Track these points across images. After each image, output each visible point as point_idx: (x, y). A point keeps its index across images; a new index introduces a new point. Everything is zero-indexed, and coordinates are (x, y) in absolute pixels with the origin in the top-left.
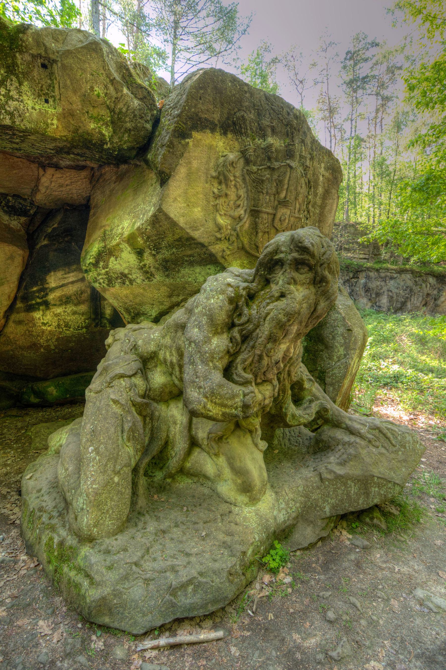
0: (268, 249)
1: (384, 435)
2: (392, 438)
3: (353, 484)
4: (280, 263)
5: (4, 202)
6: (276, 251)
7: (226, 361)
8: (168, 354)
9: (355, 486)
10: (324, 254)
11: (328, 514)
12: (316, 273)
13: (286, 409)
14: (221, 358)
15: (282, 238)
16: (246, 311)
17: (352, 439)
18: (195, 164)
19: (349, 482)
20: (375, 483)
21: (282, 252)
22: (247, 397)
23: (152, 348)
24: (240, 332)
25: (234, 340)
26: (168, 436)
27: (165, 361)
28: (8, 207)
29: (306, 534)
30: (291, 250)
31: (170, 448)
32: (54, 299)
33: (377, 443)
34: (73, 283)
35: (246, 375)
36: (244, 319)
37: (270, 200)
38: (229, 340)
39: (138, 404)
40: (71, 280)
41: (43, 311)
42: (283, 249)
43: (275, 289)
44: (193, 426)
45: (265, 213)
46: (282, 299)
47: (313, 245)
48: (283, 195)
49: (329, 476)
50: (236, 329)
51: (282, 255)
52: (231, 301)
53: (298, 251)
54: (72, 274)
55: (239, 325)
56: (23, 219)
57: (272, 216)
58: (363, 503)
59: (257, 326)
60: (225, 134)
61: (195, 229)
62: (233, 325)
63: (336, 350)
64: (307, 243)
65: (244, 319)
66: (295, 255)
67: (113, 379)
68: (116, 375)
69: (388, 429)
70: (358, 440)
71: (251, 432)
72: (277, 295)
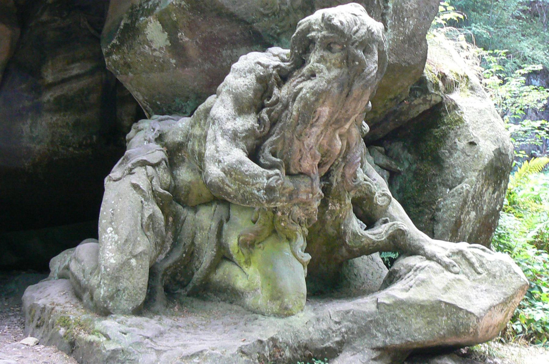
0: (301, 27)
1: (468, 260)
2: (477, 265)
4: (312, 41)
6: (309, 29)
7: (250, 142)
8: (196, 144)
11: (380, 344)
12: (348, 52)
13: (346, 225)
14: (245, 138)
15: (317, 15)
16: (276, 91)
17: (427, 263)
21: (314, 30)
22: (271, 179)
23: (179, 138)
24: (269, 113)
25: (262, 121)
26: (193, 243)
27: (193, 151)
30: (322, 28)
31: (196, 259)
32: (49, 101)
33: (456, 269)
34: (78, 77)
35: (274, 159)
36: (273, 98)
38: (256, 120)
39: (160, 195)
40: (75, 72)
42: (316, 27)
44: (224, 233)
46: (313, 78)
47: (342, 23)
49: (387, 302)
50: (264, 110)
51: (313, 34)
52: (261, 80)
53: (327, 29)
54: (78, 64)
55: (270, 105)
59: (286, 107)
62: (263, 106)
64: (336, 22)
65: (273, 98)
67: (135, 165)
68: (138, 162)
69: (474, 254)
70: (433, 264)
71: (289, 240)
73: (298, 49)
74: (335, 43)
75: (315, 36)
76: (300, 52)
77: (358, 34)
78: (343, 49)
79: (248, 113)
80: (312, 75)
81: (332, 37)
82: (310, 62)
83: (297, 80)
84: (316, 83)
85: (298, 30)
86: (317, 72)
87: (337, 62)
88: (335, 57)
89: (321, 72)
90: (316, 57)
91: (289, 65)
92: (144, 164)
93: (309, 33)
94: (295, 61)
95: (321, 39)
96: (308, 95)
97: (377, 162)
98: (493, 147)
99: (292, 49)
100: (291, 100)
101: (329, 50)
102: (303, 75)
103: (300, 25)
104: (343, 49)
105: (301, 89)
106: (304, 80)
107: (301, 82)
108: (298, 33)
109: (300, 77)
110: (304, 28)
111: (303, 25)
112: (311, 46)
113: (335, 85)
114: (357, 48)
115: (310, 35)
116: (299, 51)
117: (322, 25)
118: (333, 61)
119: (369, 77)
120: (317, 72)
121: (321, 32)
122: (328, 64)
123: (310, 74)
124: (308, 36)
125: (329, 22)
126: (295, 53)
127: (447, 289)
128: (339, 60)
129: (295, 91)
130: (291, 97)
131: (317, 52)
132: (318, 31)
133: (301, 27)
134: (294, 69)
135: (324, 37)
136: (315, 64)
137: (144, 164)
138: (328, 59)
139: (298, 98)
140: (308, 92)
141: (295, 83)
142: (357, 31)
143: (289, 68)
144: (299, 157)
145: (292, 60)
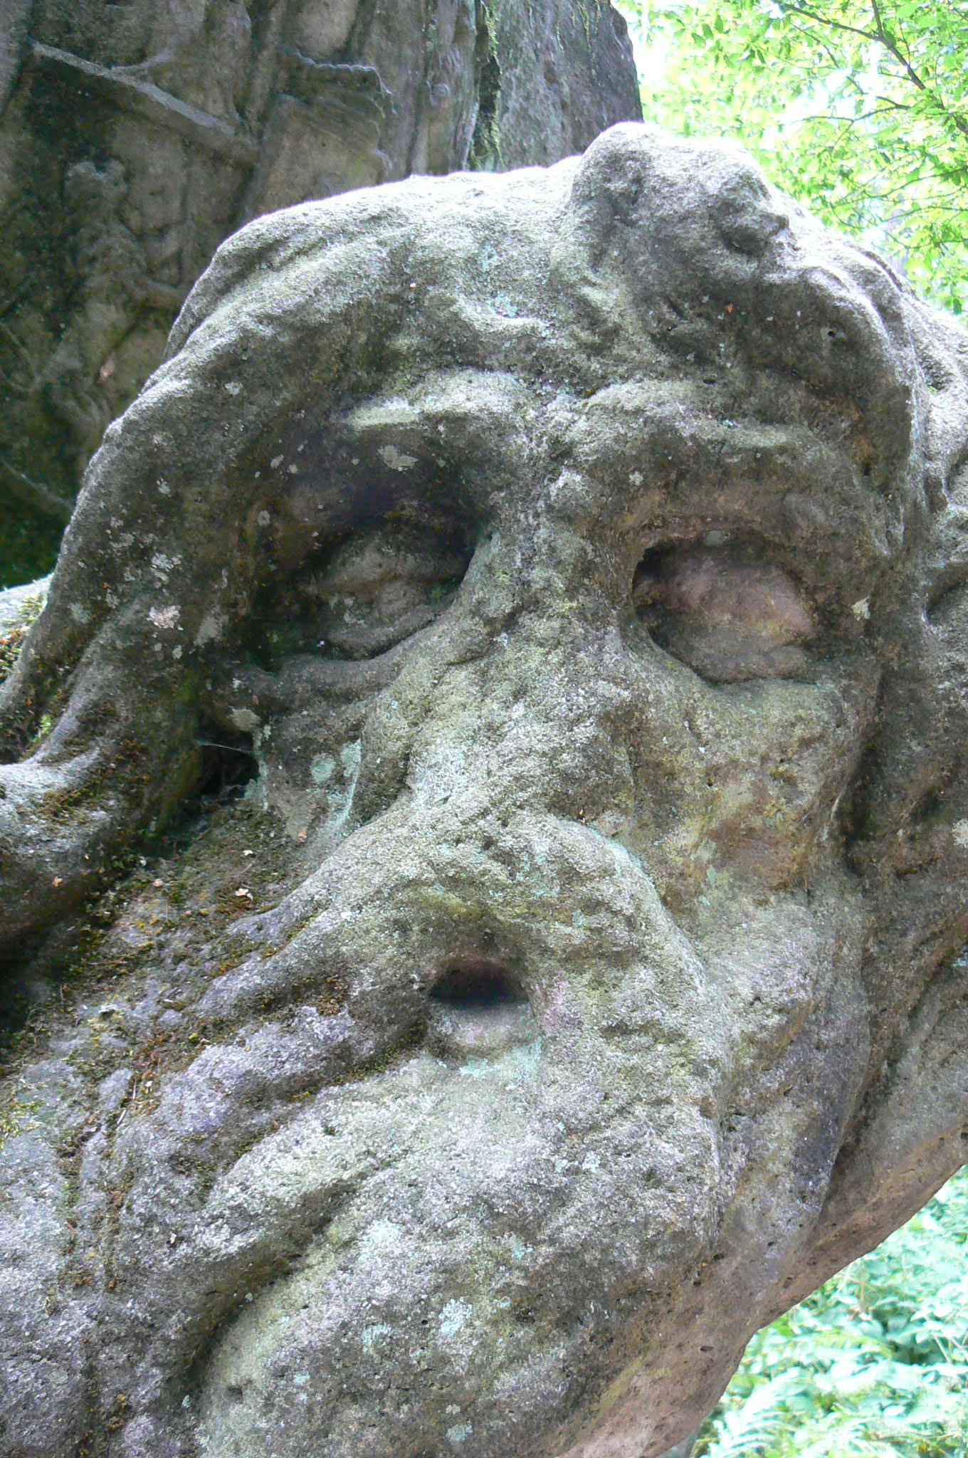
0: (277, 290)
4: (443, 510)
6: (397, 325)
21: (463, 351)
43: (353, 880)
46: (468, 1031)
53: (684, 354)
57: (227, 179)
66: (654, 396)
72: (380, 962)
73: (191, 589)
74: (748, 550)
75: (501, 427)
76: (210, 629)
78: (826, 642)
80: (473, 975)
81: (760, 463)
82: (386, 788)
83: (226, 1060)
84: (575, 1132)
85: (221, 324)
86: (574, 958)
87: (782, 814)
88: (765, 733)
89: (622, 959)
90: (528, 732)
91: (62, 805)
93: (371, 392)
94: (129, 754)
95: (607, 470)
96: (453, 1319)
99: (100, 576)
100: (150, 1383)
101: (660, 638)
102: (321, 983)
103: (258, 259)
104: (826, 642)
105: (315, 1218)
106: (343, 1066)
107: (301, 1089)
108: (227, 365)
109: (271, 1004)
110: (330, 304)
111: (310, 269)
112: (366, 563)
115: (393, 410)
116: (189, 620)
117: (608, 295)
118: (734, 797)
120: (574, 958)
121: (585, 386)
122: (685, 837)
123: (429, 966)
124: (370, 417)
125: (743, 268)
126: (143, 633)
128: (809, 788)
129: (221, 1241)
130: (139, 1336)
131: (525, 658)
132: (536, 365)
133: (277, 290)
134: (116, 863)
135: (667, 459)
136: (542, 835)
138: (689, 761)
139: (257, 1352)
140: (452, 1281)
141: (195, 1093)
143: (67, 838)
145: (92, 723)
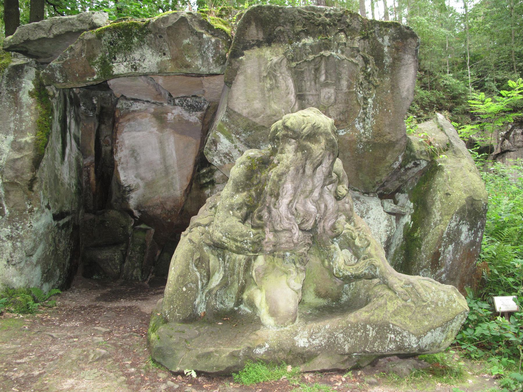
3: (371, 329)
5: (185, 103)
6: (276, 130)
9: (373, 330)
10: (304, 129)
18: (249, 71)
19: (368, 326)
20: (391, 330)
24: (256, 191)
28: (188, 106)
29: (323, 362)
37: (311, 85)
41: (211, 189)
45: (310, 95)
48: (323, 78)
56: (199, 114)
58: (378, 346)
60: (270, 45)
61: (257, 116)
63: (434, 216)
77: (305, 131)
79: (244, 190)
92: (199, 225)
97: (386, 211)
98: (465, 196)
113: (292, 168)
114: (304, 139)
119: (315, 161)
127: (395, 313)
137: (199, 225)
142: (304, 129)
144: (279, 219)
